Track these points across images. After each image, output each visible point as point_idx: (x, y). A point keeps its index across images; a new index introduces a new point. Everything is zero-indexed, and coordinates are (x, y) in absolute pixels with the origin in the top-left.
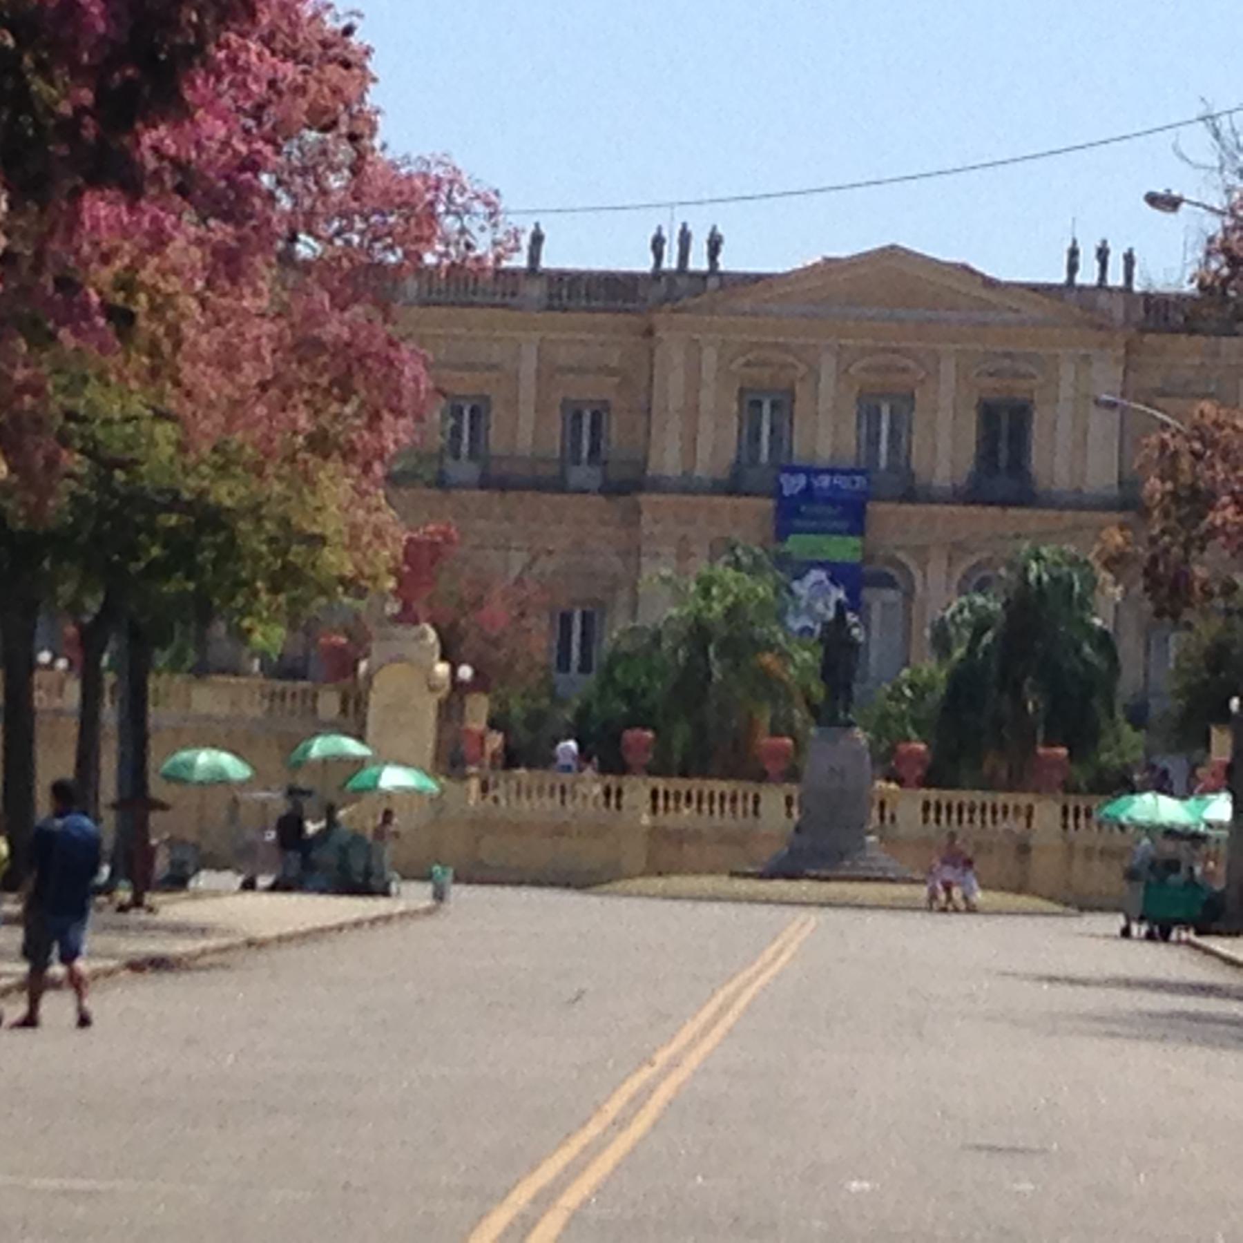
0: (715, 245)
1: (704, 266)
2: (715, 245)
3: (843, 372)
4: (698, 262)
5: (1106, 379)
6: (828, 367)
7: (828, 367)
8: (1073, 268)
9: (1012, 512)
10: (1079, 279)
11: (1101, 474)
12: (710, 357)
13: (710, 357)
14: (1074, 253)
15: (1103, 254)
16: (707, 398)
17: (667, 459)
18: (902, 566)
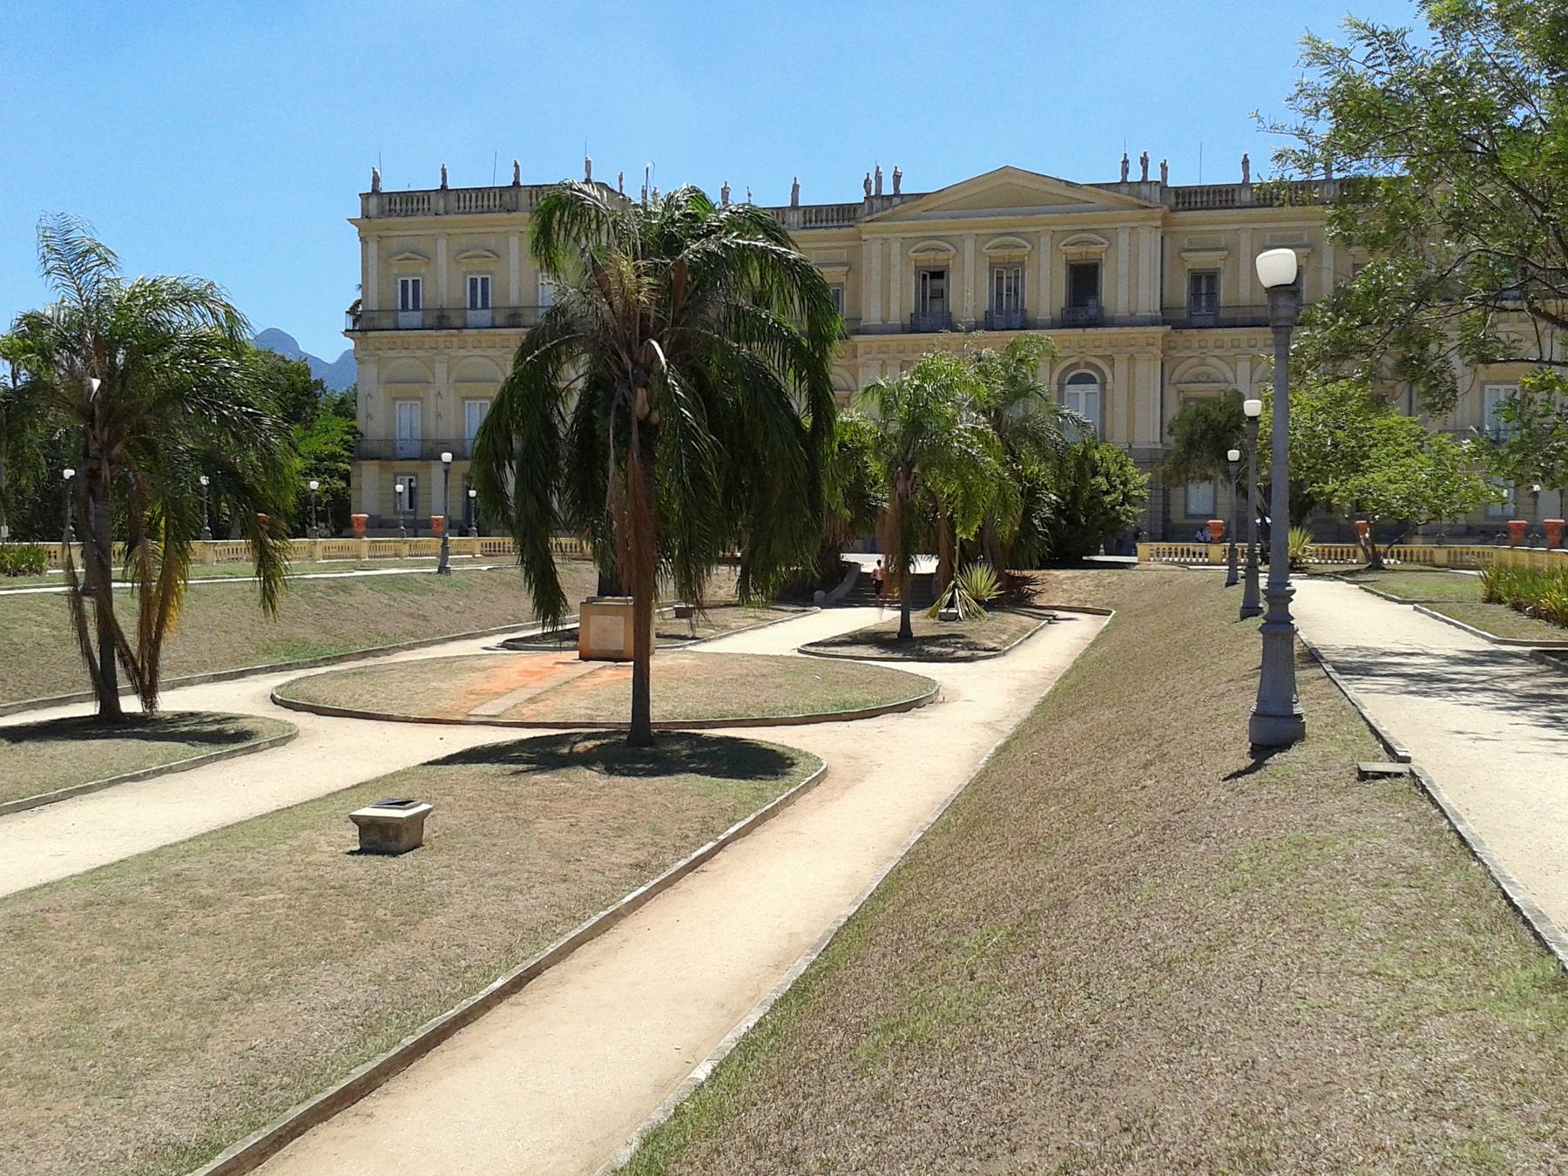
0: (897, 178)
1: (892, 192)
2: (897, 178)
3: (977, 252)
4: (888, 190)
5: (1149, 241)
6: (969, 246)
7: (969, 246)
8: (1125, 171)
9: (1089, 330)
11: (1148, 302)
13: (896, 248)
14: (1125, 162)
15: (1144, 161)
16: (895, 276)
17: (872, 313)
18: (1096, 368)
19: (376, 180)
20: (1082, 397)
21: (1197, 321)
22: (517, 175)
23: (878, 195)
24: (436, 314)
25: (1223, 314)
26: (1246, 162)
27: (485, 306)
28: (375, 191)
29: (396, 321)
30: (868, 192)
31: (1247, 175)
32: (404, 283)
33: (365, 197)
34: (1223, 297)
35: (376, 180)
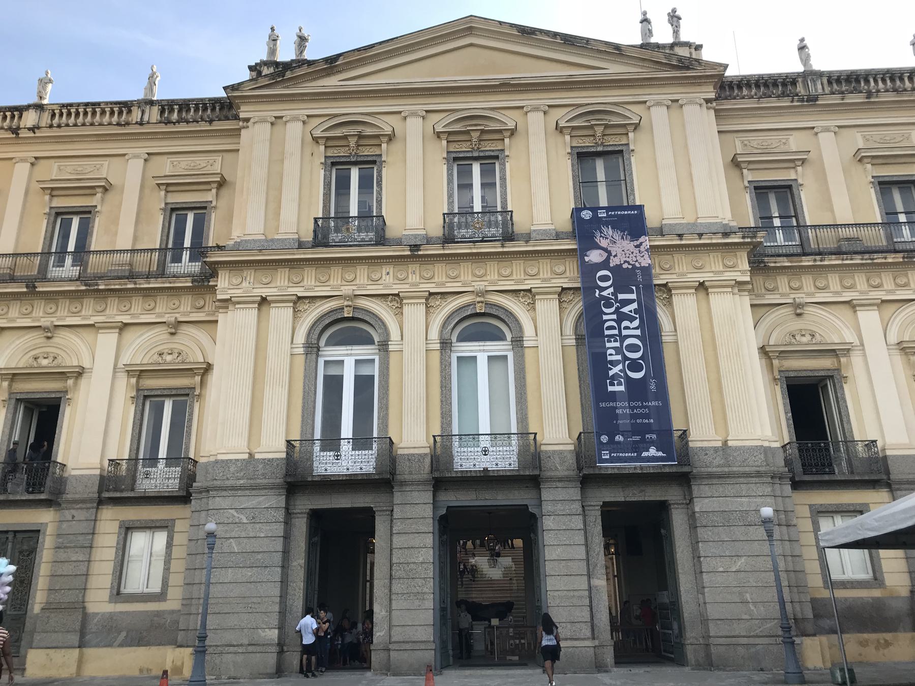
8: (647, 33)
10: (656, 39)
14: (645, 21)
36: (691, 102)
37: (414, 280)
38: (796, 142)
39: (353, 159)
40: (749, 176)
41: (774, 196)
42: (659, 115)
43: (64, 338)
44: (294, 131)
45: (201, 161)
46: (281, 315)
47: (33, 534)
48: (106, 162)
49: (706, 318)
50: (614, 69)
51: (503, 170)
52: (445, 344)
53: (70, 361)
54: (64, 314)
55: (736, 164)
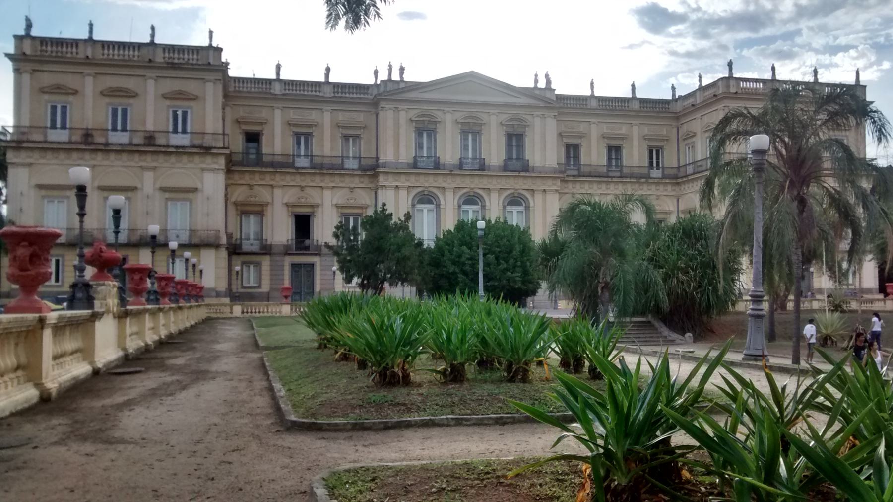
0: (402, 70)
1: (398, 79)
2: (402, 70)
4: (396, 77)
7: (449, 119)
8: (536, 82)
12: (403, 116)
16: (402, 131)
19: (29, 26)
20: (425, 211)
21: (611, 174)
22: (153, 36)
23: (389, 80)
24: (84, 132)
25: (625, 170)
26: (592, 84)
27: (184, 131)
28: (28, 35)
29: (45, 135)
30: (376, 78)
31: (593, 91)
32: (54, 108)
33: (19, 39)
34: (584, 160)
35: (29, 26)
36: (549, 116)
37: (449, 183)
38: (582, 128)
39: (426, 128)
40: (565, 140)
41: (572, 151)
42: (537, 121)
43: (308, 190)
44: (403, 116)
45: (354, 115)
46: (403, 193)
47: (312, 265)
48: (314, 112)
49: (544, 201)
50: (523, 100)
51: (480, 140)
52: (459, 206)
53: (311, 201)
54: (306, 181)
55: (560, 135)
